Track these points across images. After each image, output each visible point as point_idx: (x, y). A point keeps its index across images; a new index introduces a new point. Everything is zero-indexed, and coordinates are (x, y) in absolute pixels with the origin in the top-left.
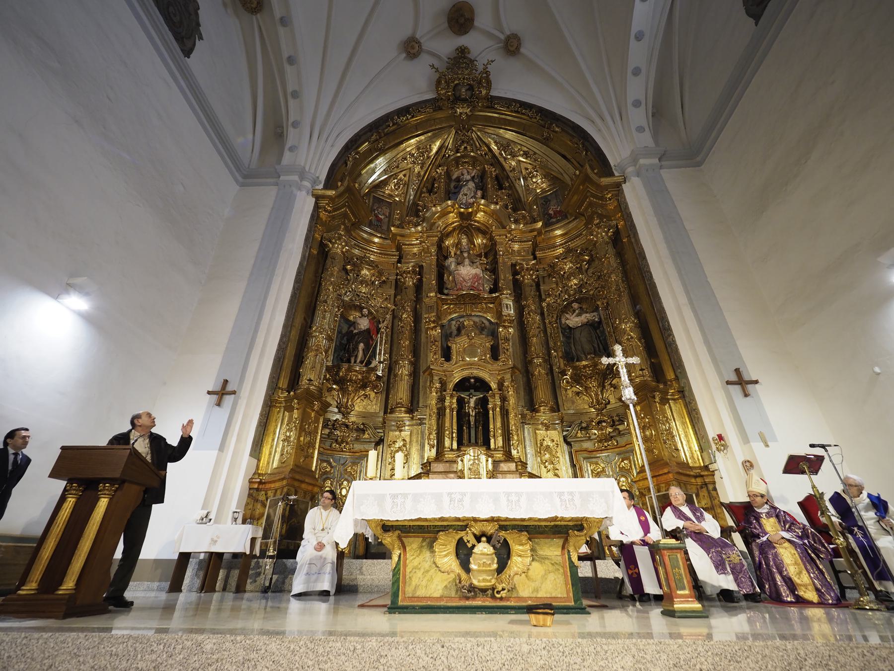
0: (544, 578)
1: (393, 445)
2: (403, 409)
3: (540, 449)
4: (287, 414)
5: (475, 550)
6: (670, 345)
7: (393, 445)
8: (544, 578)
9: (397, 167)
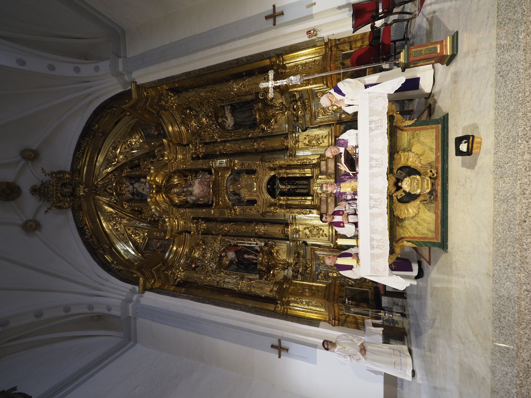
0: (423, 144)
1: (308, 235)
2: (286, 229)
3: (310, 146)
4: (291, 304)
5: (407, 190)
6: (248, 60)
7: (308, 235)
8: (423, 144)
9: (123, 235)
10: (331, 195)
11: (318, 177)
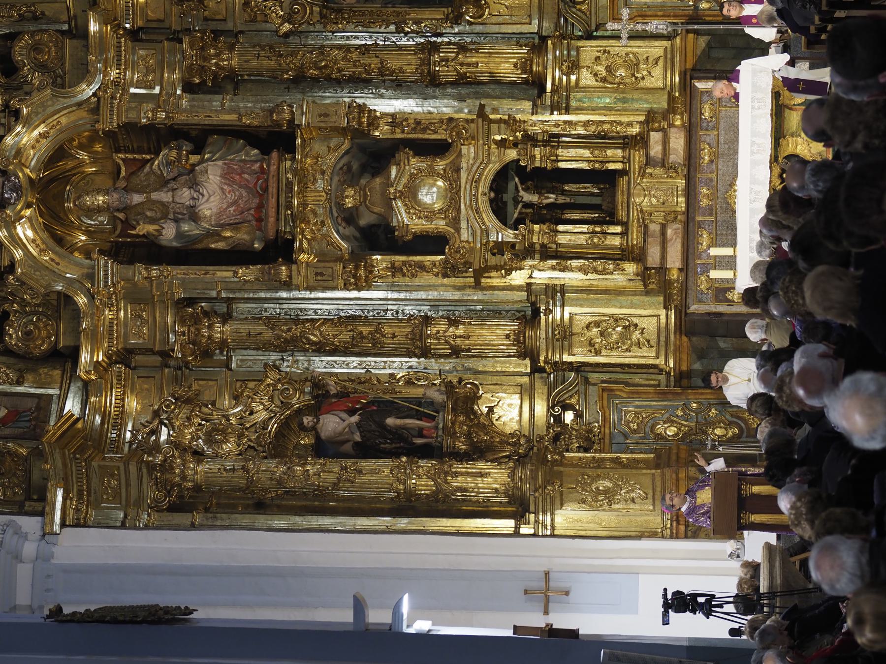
1: (597, 346)
2: (528, 333)
7: (597, 346)
10: (676, 218)
11: (644, 171)
